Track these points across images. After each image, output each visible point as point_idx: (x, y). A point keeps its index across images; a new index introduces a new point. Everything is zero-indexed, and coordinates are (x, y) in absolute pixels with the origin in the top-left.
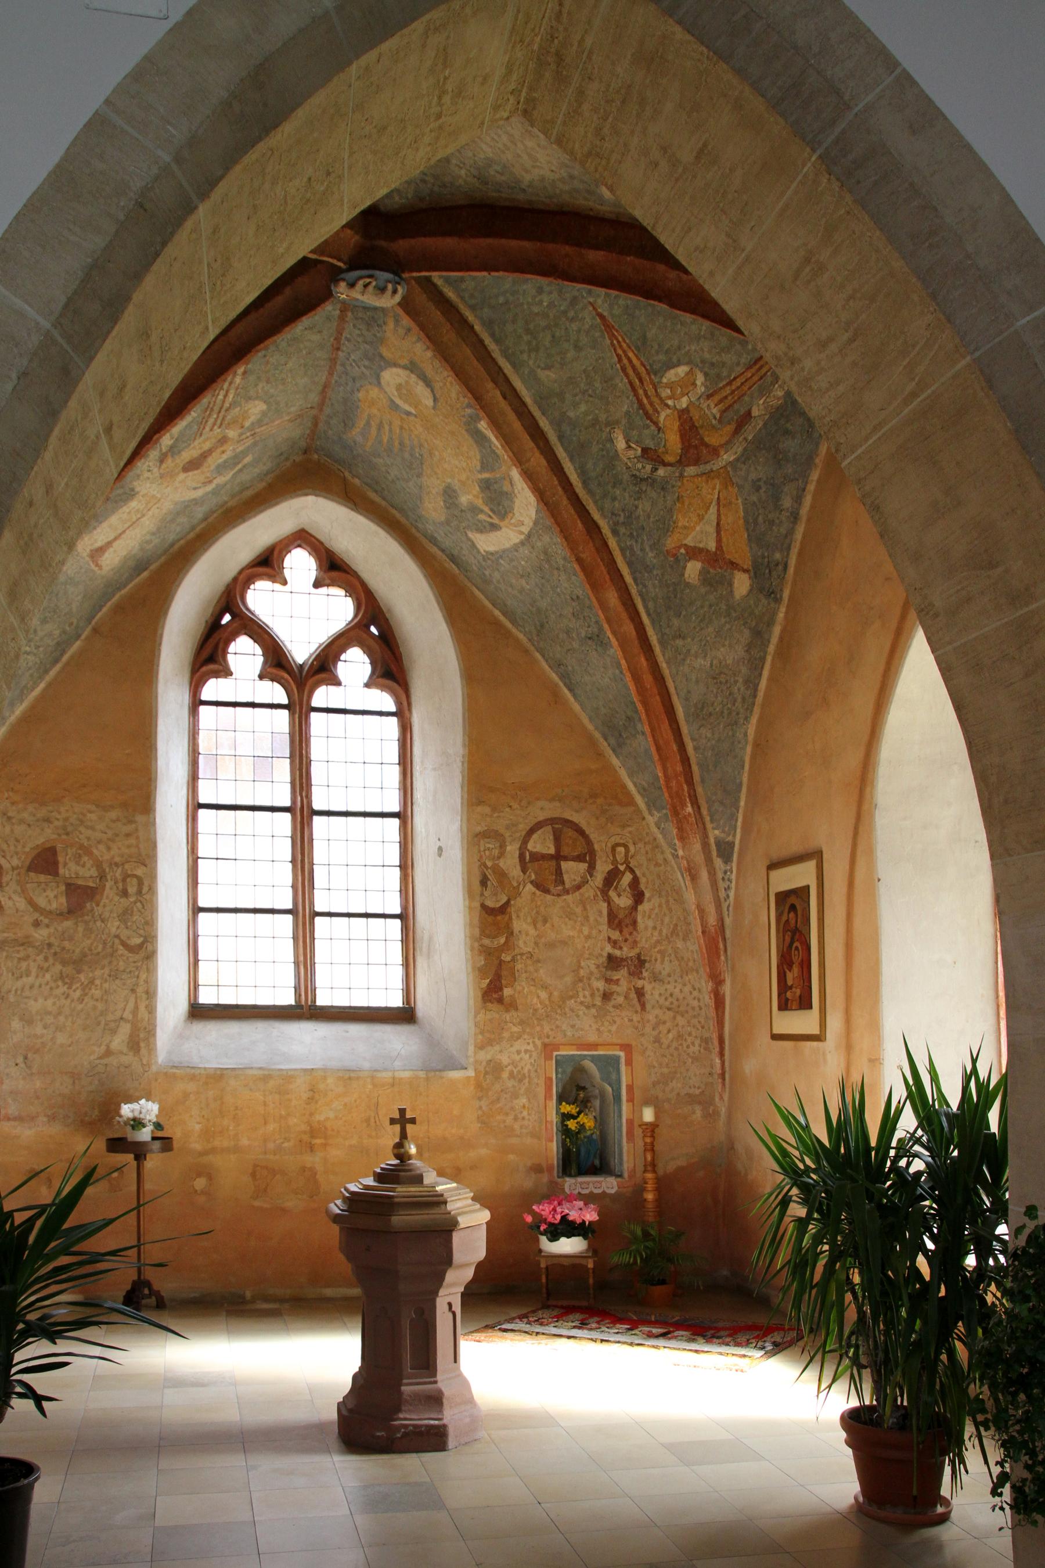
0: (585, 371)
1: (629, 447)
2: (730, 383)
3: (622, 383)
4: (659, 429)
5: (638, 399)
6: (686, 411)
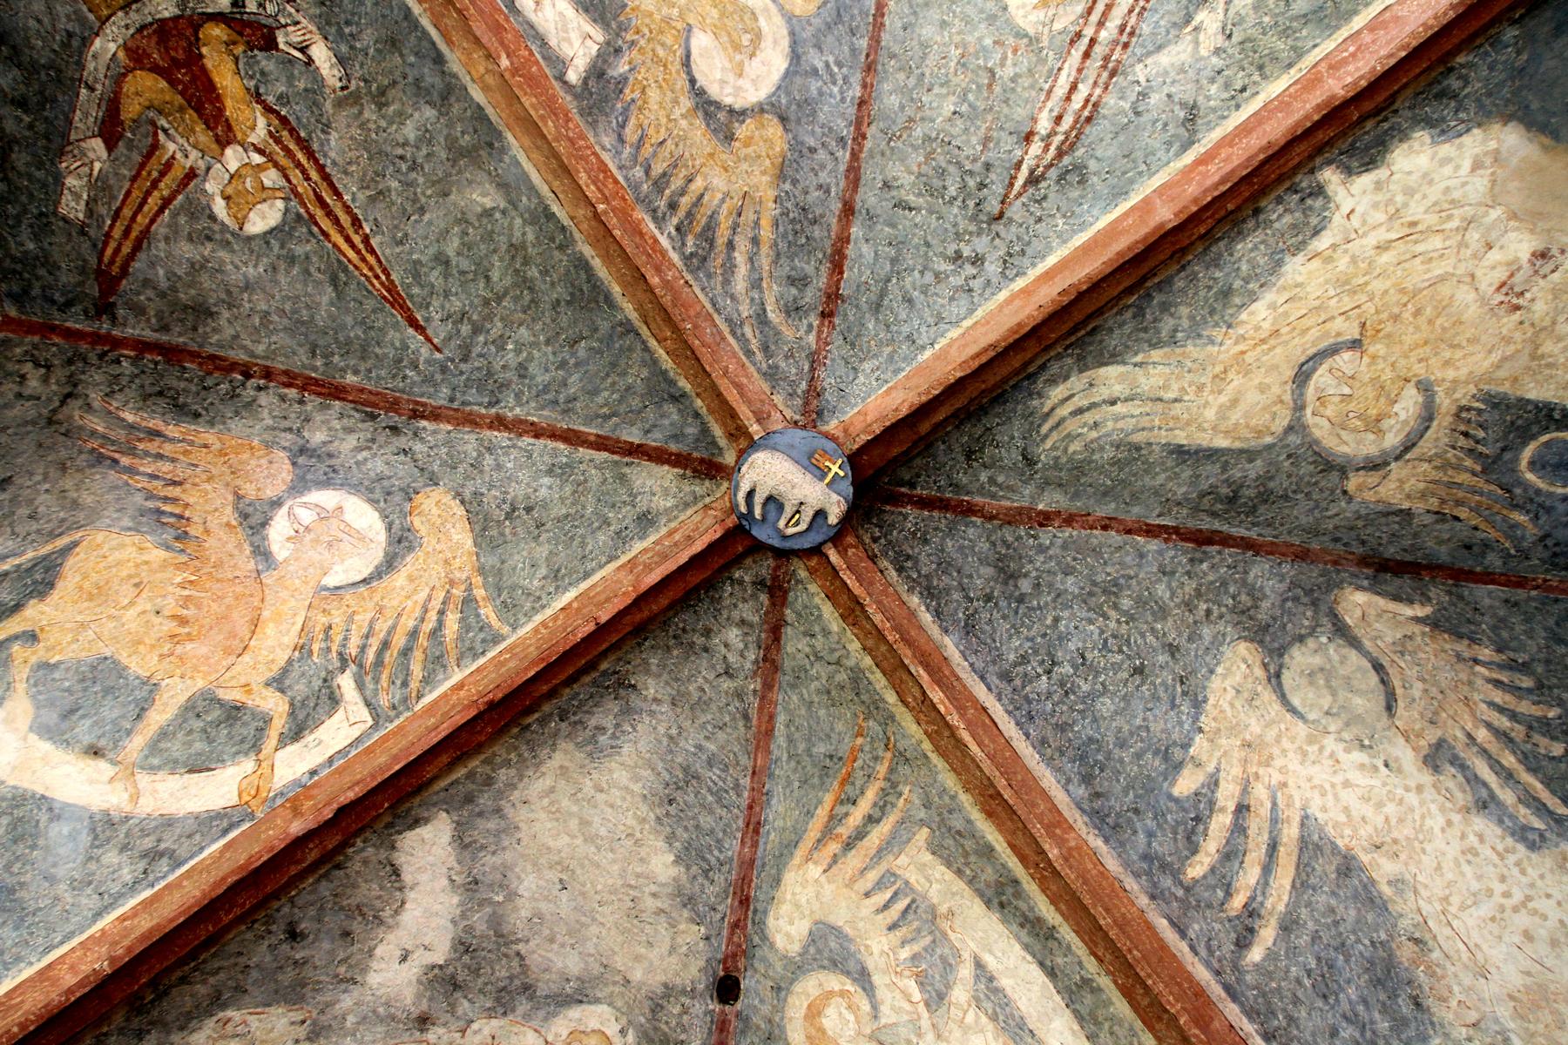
1: (303, 50)
2: (166, 202)
3: (352, 191)
4: (258, 97)
5: (316, 161)
6: (224, 141)
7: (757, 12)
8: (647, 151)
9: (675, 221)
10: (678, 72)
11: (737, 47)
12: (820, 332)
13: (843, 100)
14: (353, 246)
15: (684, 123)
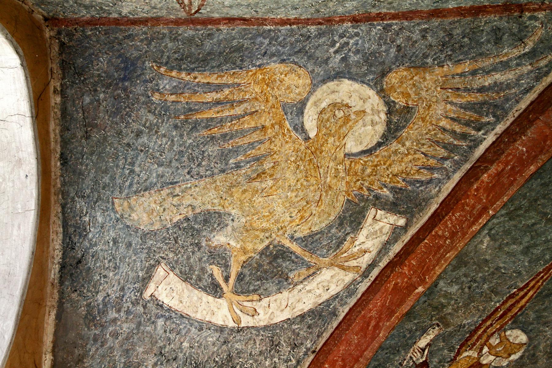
0: (498, 268)
1: (423, 350)
5: (481, 325)
7: (319, 110)
8: (432, 162)
9: (473, 132)
10: (377, 156)
11: (347, 119)
12: (535, 10)
13: (357, 34)
14: (526, 294)
15: (408, 144)
